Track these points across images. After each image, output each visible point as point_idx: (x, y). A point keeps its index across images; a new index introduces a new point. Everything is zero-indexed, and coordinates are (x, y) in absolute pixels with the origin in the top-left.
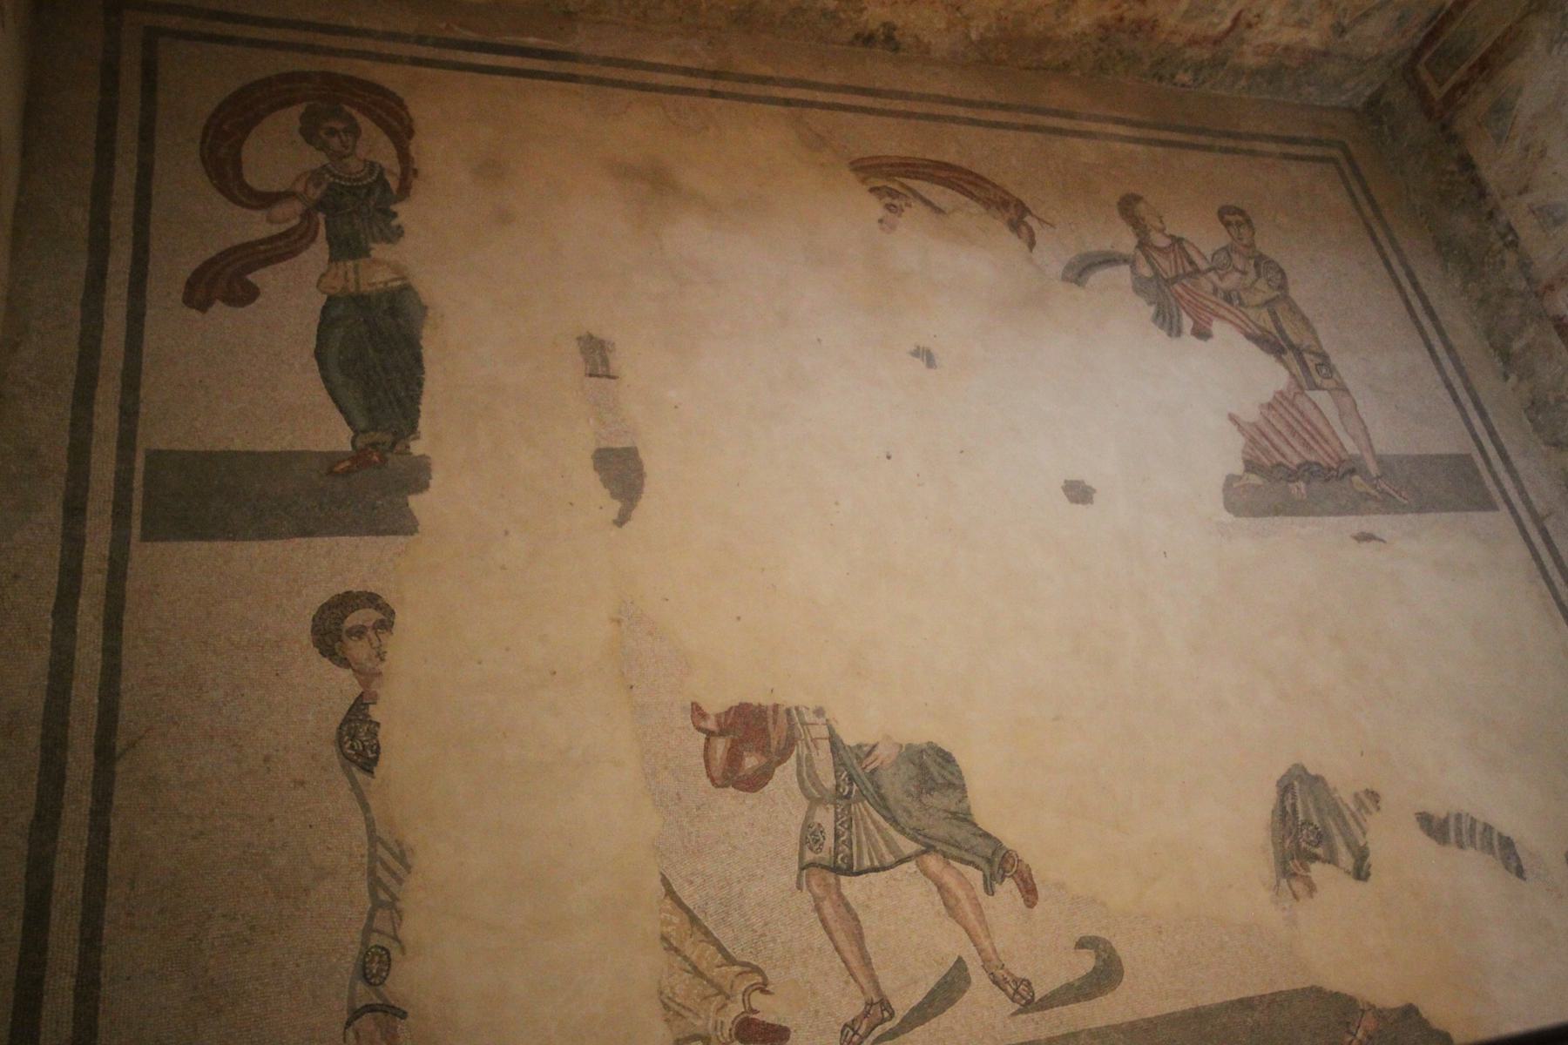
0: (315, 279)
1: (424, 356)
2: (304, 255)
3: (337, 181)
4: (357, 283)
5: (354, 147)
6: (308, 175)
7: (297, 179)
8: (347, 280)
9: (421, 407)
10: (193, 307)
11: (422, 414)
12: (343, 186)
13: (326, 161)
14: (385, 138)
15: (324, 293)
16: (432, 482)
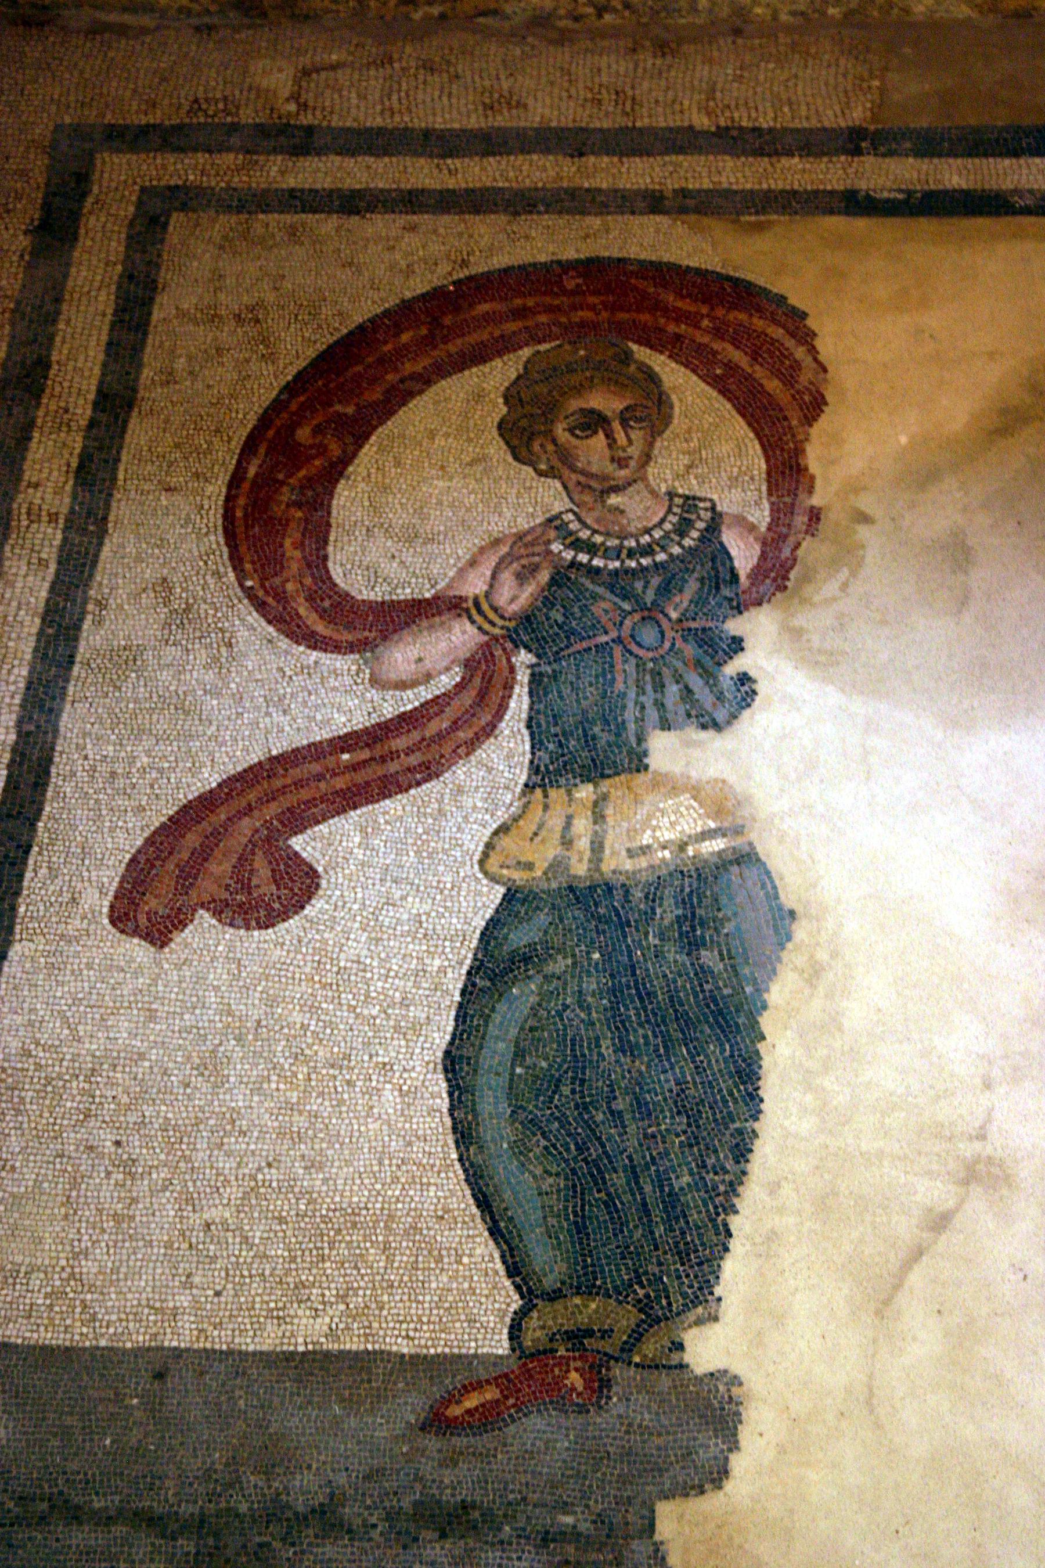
0: (475, 839)
1: (766, 1062)
2: (460, 772)
3: (583, 558)
4: (597, 847)
5: (647, 458)
6: (504, 549)
7: (473, 563)
8: (567, 842)
9: (735, 1223)
10: (136, 932)
11: (734, 1244)
12: (598, 571)
13: (560, 504)
14: (740, 427)
15: (494, 879)
16: (739, 1463)
